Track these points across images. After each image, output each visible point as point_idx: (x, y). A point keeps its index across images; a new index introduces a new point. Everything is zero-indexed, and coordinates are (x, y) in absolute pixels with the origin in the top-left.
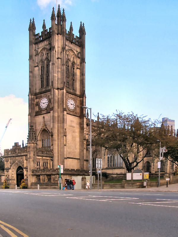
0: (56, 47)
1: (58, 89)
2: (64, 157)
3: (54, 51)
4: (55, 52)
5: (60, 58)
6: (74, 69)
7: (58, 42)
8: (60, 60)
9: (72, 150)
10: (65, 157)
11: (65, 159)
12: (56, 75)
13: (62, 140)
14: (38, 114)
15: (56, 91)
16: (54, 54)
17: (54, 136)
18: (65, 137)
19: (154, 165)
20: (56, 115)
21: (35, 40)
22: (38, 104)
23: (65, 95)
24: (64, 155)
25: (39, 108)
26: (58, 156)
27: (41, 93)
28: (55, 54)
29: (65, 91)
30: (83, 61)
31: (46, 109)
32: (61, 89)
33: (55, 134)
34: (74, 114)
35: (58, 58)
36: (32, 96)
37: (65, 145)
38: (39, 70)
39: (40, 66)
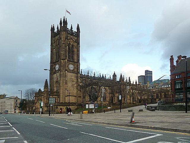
0: (62, 38)
1: (63, 60)
4: (62, 40)
6: (73, 48)
7: (63, 35)
8: (64, 44)
10: (66, 95)
14: (55, 73)
17: (60, 85)
18: (66, 85)
19: (114, 99)
20: (62, 73)
21: (54, 34)
22: (55, 68)
23: (66, 62)
25: (55, 70)
27: (56, 62)
28: (62, 42)
29: (66, 60)
30: (78, 44)
31: (58, 70)
32: (64, 60)
34: (73, 72)
35: (63, 44)
37: (66, 89)
38: (55, 50)
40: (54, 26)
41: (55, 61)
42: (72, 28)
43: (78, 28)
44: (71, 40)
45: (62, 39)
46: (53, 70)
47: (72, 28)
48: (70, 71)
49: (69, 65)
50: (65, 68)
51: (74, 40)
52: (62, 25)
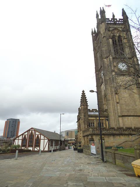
2: (118, 115)
3: (100, 35)
4: (101, 34)
5: (105, 37)
8: (104, 38)
9: (130, 107)
11: (119, 117)
12: (104, 49)
13: (115, 99)
15: (105, 60)
16: (100, 36)
18: (117, 96)
24: (118, 113)
26: (114, 114)
33: (108, 95)
36: (97, 72)
37: (118, 103)
39: (99, 51)
40: (95, 29)
41: (100, 68)
42: (114, 16)
43: (124, 13)
44: (116, 31)
45: (102, 33)
46: (99, 80)
47: (114, 16)
48: (121, 73)
49: (118, 64)
50: (111, 69)
51: (120, 29)
52: (100, 17)
